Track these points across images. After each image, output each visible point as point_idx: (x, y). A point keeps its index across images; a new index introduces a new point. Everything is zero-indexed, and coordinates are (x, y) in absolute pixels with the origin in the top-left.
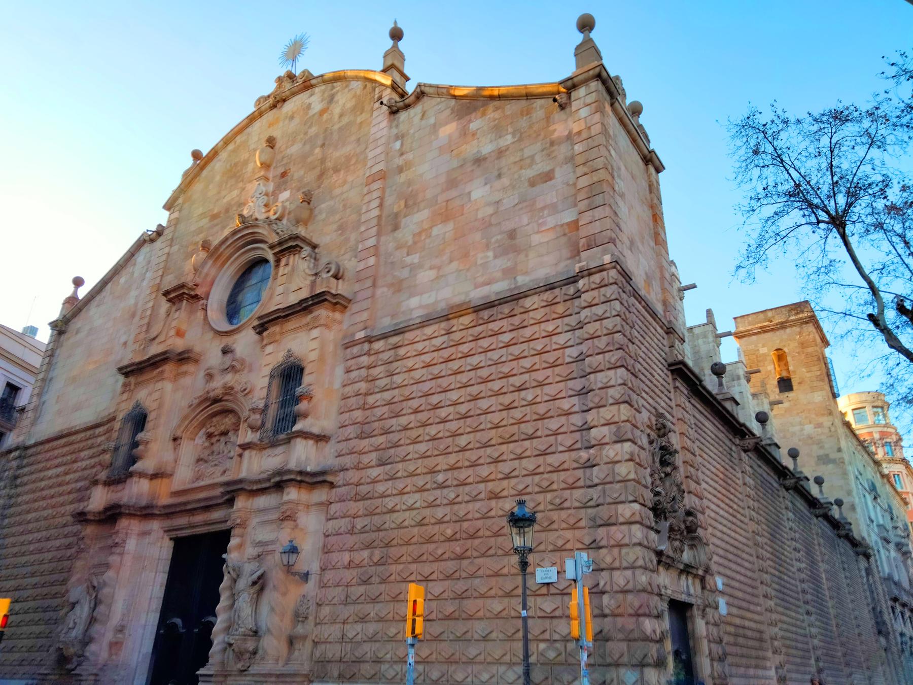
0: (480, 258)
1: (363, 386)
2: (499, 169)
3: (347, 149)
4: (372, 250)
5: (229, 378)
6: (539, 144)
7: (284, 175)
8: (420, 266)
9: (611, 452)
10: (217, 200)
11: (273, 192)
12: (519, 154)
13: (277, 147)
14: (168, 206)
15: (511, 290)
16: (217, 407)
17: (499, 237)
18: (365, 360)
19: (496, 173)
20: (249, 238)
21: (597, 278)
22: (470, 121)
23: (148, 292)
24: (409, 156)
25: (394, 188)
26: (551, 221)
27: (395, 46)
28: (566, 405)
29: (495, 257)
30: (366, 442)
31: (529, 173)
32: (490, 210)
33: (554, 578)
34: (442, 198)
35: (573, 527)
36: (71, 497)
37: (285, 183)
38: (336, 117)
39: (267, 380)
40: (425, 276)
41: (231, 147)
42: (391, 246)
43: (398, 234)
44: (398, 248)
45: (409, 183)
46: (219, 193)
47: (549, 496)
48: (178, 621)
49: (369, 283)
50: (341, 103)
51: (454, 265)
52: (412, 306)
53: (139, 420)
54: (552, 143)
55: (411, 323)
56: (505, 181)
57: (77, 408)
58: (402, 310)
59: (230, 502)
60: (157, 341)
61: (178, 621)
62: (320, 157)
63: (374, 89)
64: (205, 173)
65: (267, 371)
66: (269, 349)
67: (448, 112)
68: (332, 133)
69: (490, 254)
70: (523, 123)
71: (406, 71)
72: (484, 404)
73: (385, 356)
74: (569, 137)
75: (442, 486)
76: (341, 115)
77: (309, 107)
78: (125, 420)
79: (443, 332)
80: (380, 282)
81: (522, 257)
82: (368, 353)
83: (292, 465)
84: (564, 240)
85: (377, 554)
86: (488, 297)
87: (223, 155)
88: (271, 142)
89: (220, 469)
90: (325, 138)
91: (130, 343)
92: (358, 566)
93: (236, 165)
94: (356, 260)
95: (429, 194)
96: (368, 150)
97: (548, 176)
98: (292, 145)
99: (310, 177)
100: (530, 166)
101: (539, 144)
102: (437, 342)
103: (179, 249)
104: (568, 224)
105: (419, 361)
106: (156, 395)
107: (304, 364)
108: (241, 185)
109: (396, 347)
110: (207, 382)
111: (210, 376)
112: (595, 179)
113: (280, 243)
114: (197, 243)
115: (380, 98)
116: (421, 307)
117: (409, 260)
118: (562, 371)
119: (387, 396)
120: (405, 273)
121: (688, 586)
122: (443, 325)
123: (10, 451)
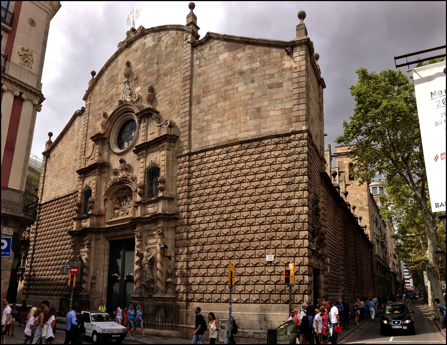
0: (242, 119)
4: (188, 113)
8: (212, 121)
25: (197, 83)
27: (192, 12)
29: (250, 119)
34: (222, 89)
40: (215, 126)
43: (201, 106)
44: (200, 112)
45: (205, 81)
49: (187, 128)
51: (230, 121)
52: (209, 139)
55: (209, 147)
63: (183, 34)
67: (223, 47)
69: (248, 117)
79: (225, 152)
80: (193, 128)
94: (180, 118)
95: (215, 87)
96: (182, 65)
109: (202, 158)
115: (186, 39)
116: (213, 140)
117: (206, 118)
119: (199, 179)
120: (205, 124)
122: (224, 149)
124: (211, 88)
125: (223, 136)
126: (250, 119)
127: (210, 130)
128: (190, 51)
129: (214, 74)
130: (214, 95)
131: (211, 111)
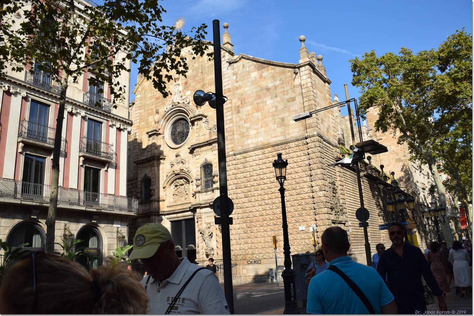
1: (235, 171)
5: (181, 165)
11: (183, 91)
15: (284, 140)
16: (178, 176)
18: (234, 162)
21: (312, 139)
24: (240, 83)
29: (278, 127)
31: (287, 97)
32: (274, 109)
34: (255, 102)
37: (188, 87)
40: (252, 132)
43: (240, 114)
47: (301, 206)
48: (180, 247)
51: (263, 129)
54: (294, 87)
56: (278, 99)
59: (194, 210)
62: (201, 77)
65: (199, 165)
66: (197, 157)
67: (253, 67)
69: (276, 126)
70: (283, 76)
73: (242, 161)
74: (301, 85)
75: (267, 204)
78: (141, 182)
80: (235, 133)
86: (276, 142)
89: (183, 199)
95: (250, 100)
102: (261, 156)
105: (254, 163)
106: (153, 172)
107: (213, 163)
111: (172, 165)
112: (310, 103)
113: (194, 117)
114: (152, 109)
116: (252, 143)
117: (245, 125)
119: (244, 174)
120: (245, 130)
122: (261, 150)
124: (247, 101)
125: (259, 140)
126: (278, 127)
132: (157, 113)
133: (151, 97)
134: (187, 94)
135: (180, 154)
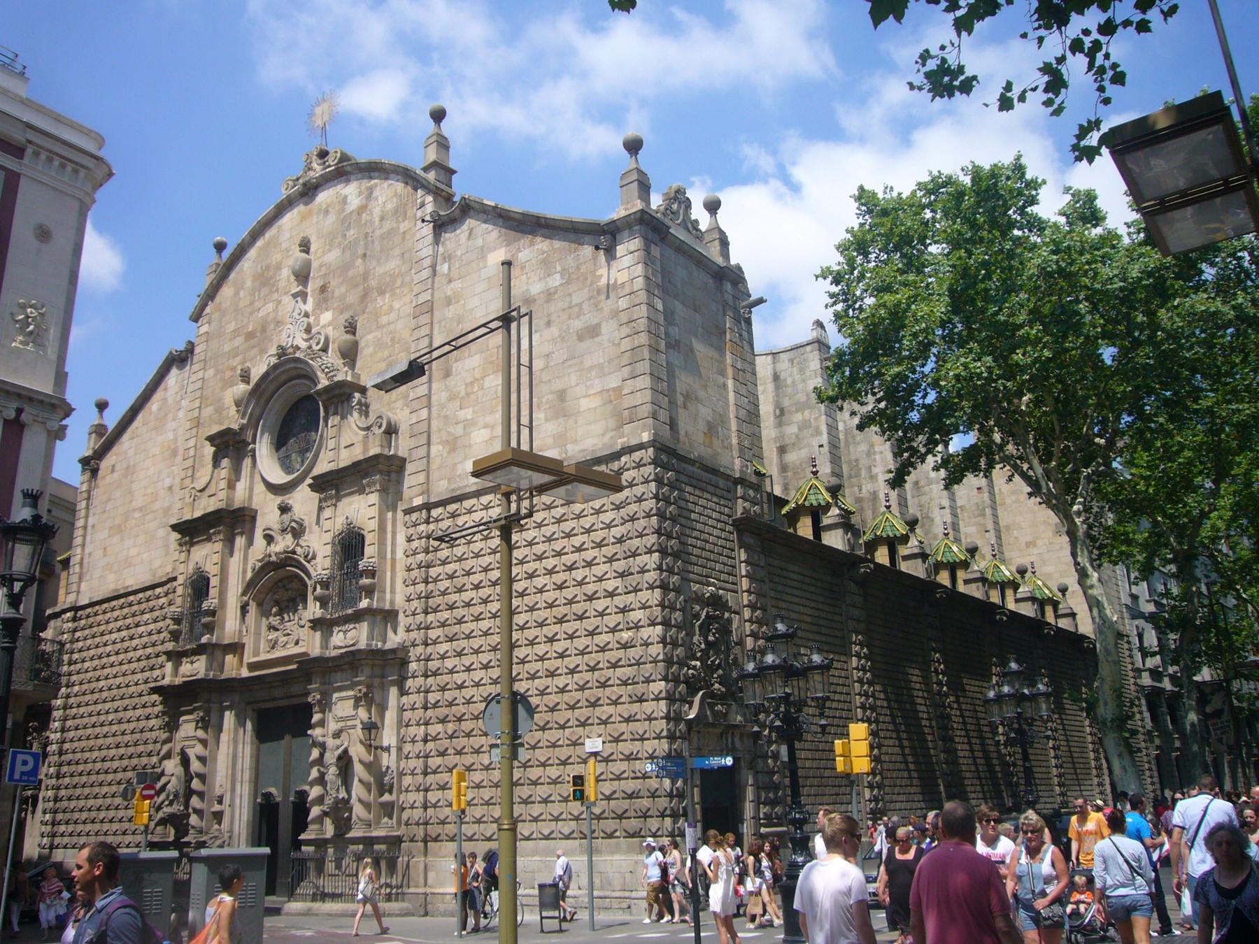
2: (549, 315)
3: (392, 265)
4: (424, 401)
6: (586, 290)
7: (323, 289)
9: (646, 633)
10: (251, 314)
12: (568, 299)
13: (312, 249)
14: (196, 317)
16: (281, 573)
17: (550, 397)
19: (546, 320)
20: (294, 373)
21: (637, 455)
22: (519, 250)
23: (188, 425)
24: (457, 285)
26: (598, 385)
28: (610, 585)
29: (547, 420)
30: (430, 617)
31: (577, 324)
33: (600, 748)
35: (615, 703)
36: (143, 663)
37: (325, 300)
38: (377, 219)
39: (329, 547)
41: (259, 243)
42: (444, 395)
43: (451, 382)
46: (252, 304)
50: (380, 200)
53: (200, 586)
56: (554, 331)
57: (128, 563)
58: (459, 472)
60: (208, 492)
61: (273, 790)
64: (233, 275)
65: (328, 537)
68: (373, 242)
70: (570, 261)
71: (452, 165)
72: (539, 582)
76: (382, 219)
77: (344, 201)
80: (434, 439)
81: (571, 422)
82: (427, 522)
83: (362, 645)
84: (609, 407)
85: (451, 727)
87: (252, 253)
88: (305, 246)
90: (366, 246)
91: (177, 488)
92: (435, 739)
93: (268, 268)
97: (593, 331)
98: (330, 251)
99: (352, 298)
100: (578, 316)
101: (586, 290)
103: (215, 375)
104: (614, 389)
107: (365, 533)
108: (276, 296)
109: (454, 515)
110: (269, 544)
111: (269, 539)
112: (636, 343)
114: (234, 369)
115: (423, 205)
118: (608, 551)
119: (449, 568)
120: (459, 430)
121: (733, 743)
123: (64, 611)
126: (547, 420)
127: (470, 446)
128: (430, 238)
129: (475, 301)
130: (477, 356)
131: (473, 397)
132: (245, 377)
133: (236, 333)
134: (322, 322)
135: (290, 502)
